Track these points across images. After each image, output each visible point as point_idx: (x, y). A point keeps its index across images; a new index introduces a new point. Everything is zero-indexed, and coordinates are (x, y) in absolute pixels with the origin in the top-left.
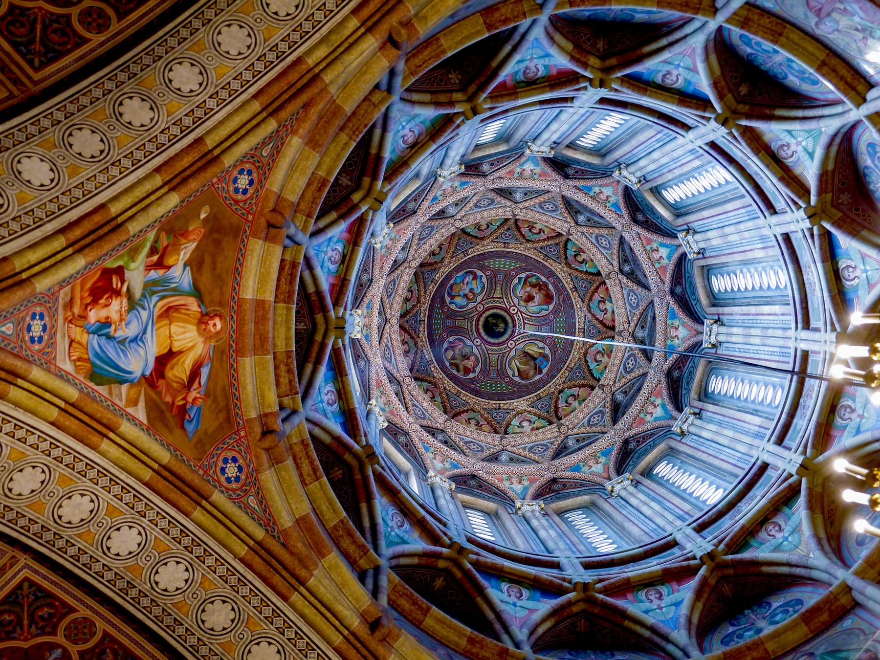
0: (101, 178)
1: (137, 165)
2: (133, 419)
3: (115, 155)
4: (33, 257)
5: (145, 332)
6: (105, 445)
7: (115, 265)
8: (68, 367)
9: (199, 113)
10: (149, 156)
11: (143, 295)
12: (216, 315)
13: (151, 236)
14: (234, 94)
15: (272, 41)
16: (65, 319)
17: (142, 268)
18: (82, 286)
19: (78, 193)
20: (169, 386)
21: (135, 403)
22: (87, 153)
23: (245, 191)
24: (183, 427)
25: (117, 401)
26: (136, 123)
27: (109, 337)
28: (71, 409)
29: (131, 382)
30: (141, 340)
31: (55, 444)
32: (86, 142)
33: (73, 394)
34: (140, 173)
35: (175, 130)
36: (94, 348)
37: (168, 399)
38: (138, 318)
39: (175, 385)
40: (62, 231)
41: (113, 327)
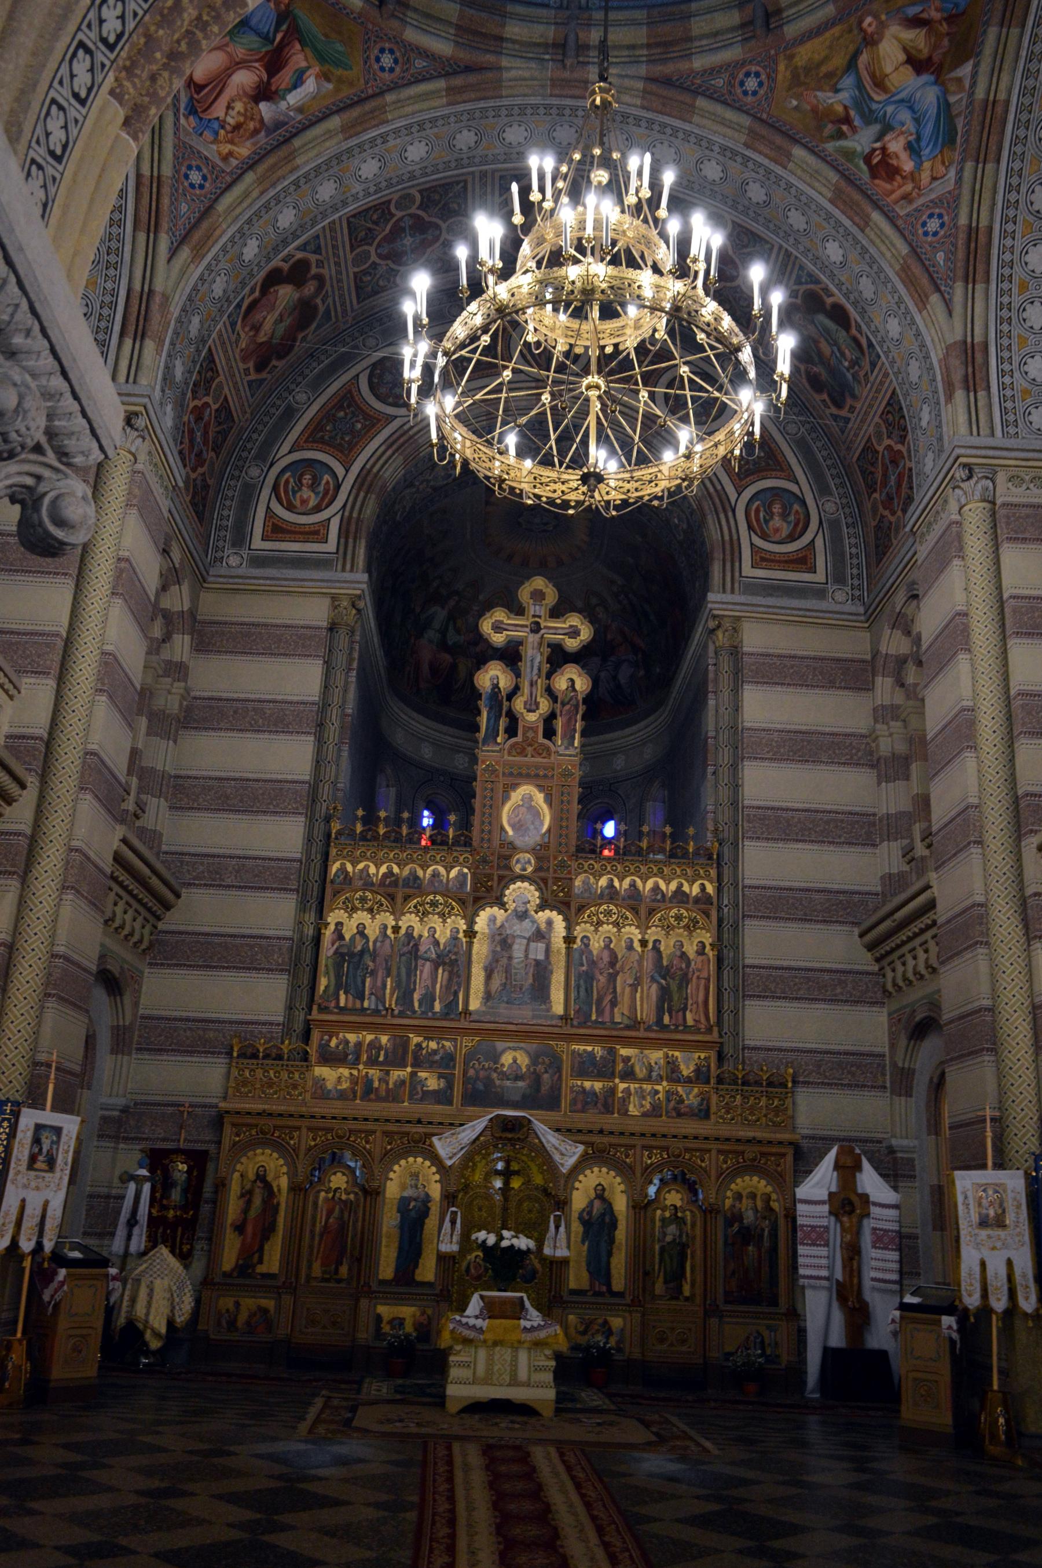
0: (813, 207)
1: (789, 186)
2: (974, 75)
3: (793, 201)
4: (888, 255)
5: (902, 101)
6: (1002, 96)
7: (864, 168)
8: (952, 173)
9: (728, 154)
10: (778, 178)
11: (876, 121)
12: (861, 30)
13: (830, 146)
14: (699, 139)
15: (647, 132)
16: (919, 195)
17: (857, 137)
18: (893, 192)
19: (832, 221)
20: (935, 47)
21: (959, 80)
22: (803, 219)
23: (757, 75)
24: (963, 13)
25: (964, 102)
26: (764, 191)
27: (918, 139)
28: (982, 156)
29: (945, 92)
30: (909, 101)
31: (1016, 141)
32: (797, 220)
33: (969, 165)
34: (793, 180)
35: (750, 164)
36: (932, 151)
37: (946, 42)
38: (894, 115)
39: (933, 40)
40: (863, 231)
41: (910, 138)
